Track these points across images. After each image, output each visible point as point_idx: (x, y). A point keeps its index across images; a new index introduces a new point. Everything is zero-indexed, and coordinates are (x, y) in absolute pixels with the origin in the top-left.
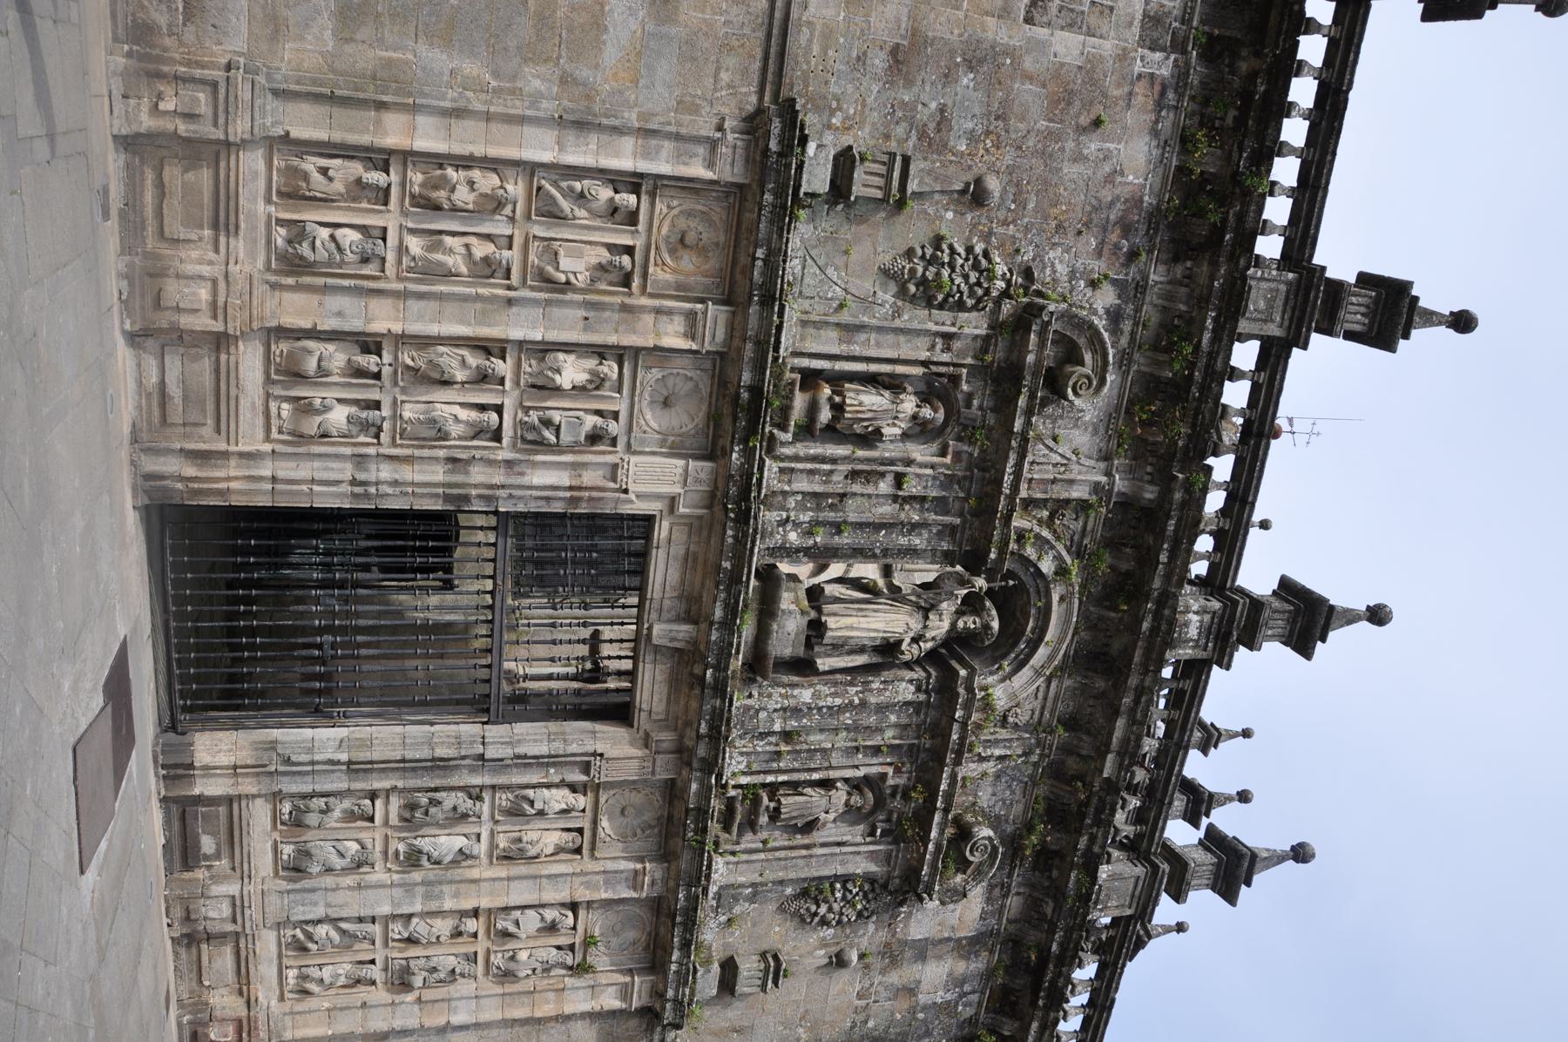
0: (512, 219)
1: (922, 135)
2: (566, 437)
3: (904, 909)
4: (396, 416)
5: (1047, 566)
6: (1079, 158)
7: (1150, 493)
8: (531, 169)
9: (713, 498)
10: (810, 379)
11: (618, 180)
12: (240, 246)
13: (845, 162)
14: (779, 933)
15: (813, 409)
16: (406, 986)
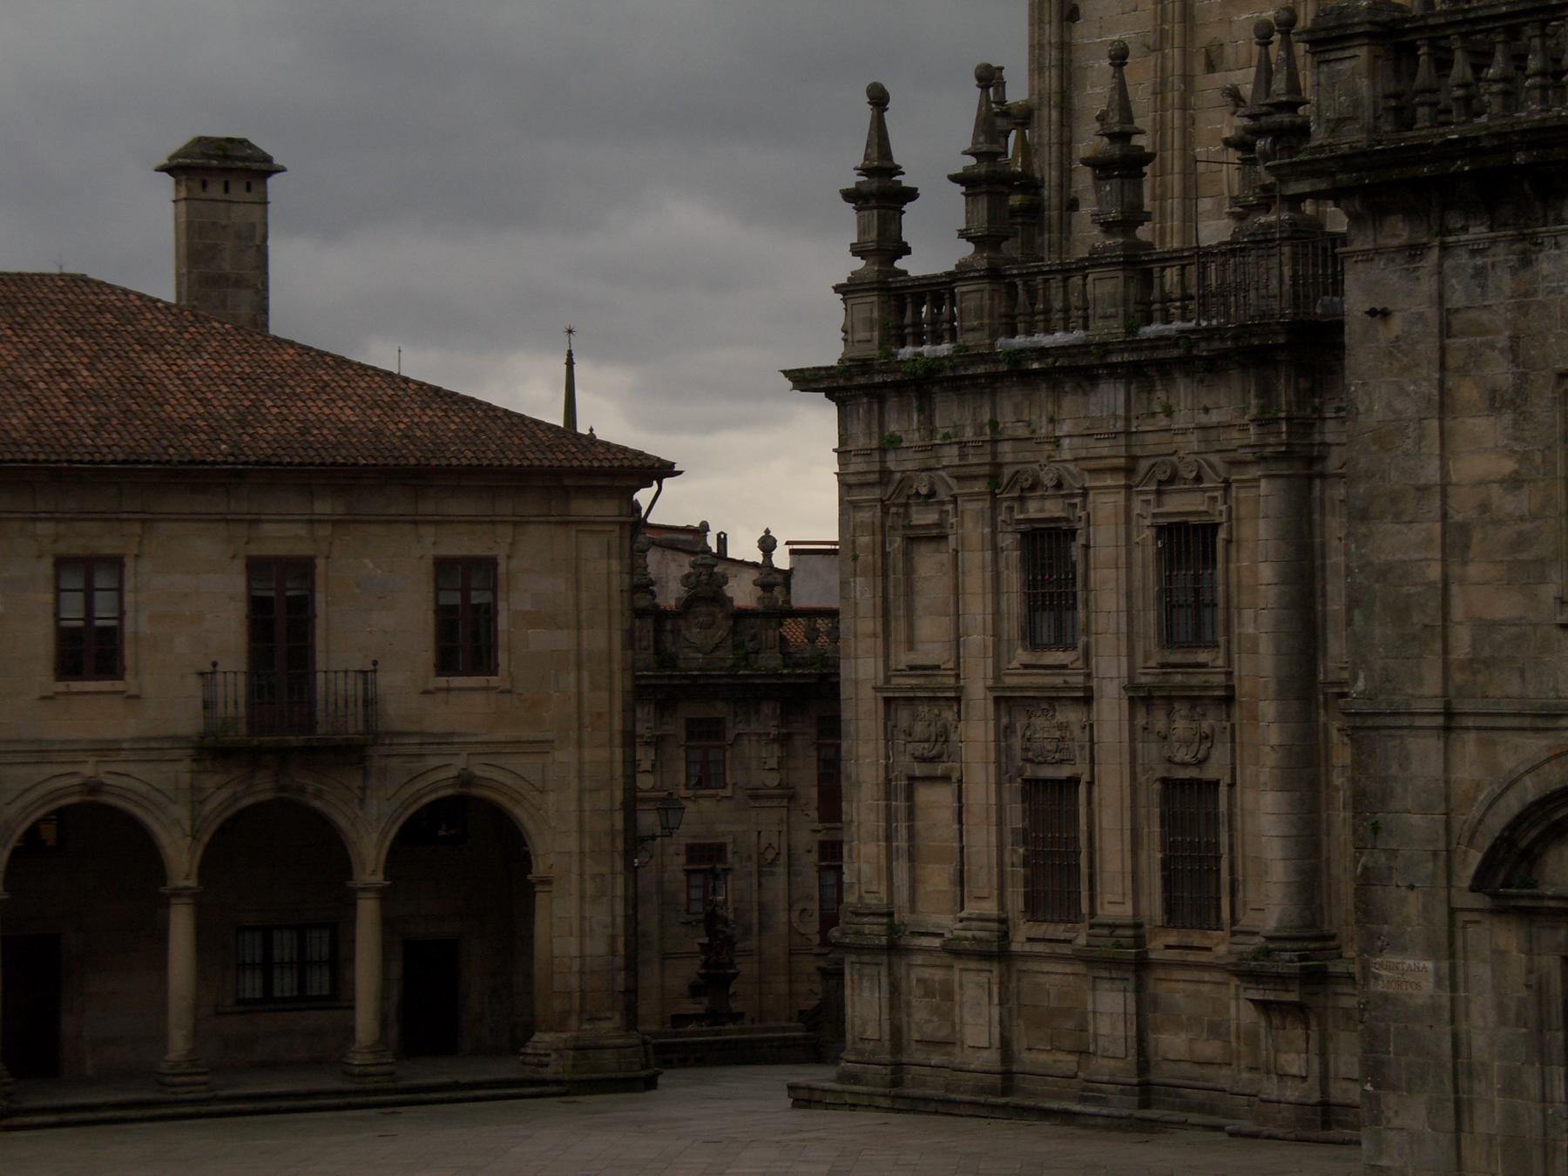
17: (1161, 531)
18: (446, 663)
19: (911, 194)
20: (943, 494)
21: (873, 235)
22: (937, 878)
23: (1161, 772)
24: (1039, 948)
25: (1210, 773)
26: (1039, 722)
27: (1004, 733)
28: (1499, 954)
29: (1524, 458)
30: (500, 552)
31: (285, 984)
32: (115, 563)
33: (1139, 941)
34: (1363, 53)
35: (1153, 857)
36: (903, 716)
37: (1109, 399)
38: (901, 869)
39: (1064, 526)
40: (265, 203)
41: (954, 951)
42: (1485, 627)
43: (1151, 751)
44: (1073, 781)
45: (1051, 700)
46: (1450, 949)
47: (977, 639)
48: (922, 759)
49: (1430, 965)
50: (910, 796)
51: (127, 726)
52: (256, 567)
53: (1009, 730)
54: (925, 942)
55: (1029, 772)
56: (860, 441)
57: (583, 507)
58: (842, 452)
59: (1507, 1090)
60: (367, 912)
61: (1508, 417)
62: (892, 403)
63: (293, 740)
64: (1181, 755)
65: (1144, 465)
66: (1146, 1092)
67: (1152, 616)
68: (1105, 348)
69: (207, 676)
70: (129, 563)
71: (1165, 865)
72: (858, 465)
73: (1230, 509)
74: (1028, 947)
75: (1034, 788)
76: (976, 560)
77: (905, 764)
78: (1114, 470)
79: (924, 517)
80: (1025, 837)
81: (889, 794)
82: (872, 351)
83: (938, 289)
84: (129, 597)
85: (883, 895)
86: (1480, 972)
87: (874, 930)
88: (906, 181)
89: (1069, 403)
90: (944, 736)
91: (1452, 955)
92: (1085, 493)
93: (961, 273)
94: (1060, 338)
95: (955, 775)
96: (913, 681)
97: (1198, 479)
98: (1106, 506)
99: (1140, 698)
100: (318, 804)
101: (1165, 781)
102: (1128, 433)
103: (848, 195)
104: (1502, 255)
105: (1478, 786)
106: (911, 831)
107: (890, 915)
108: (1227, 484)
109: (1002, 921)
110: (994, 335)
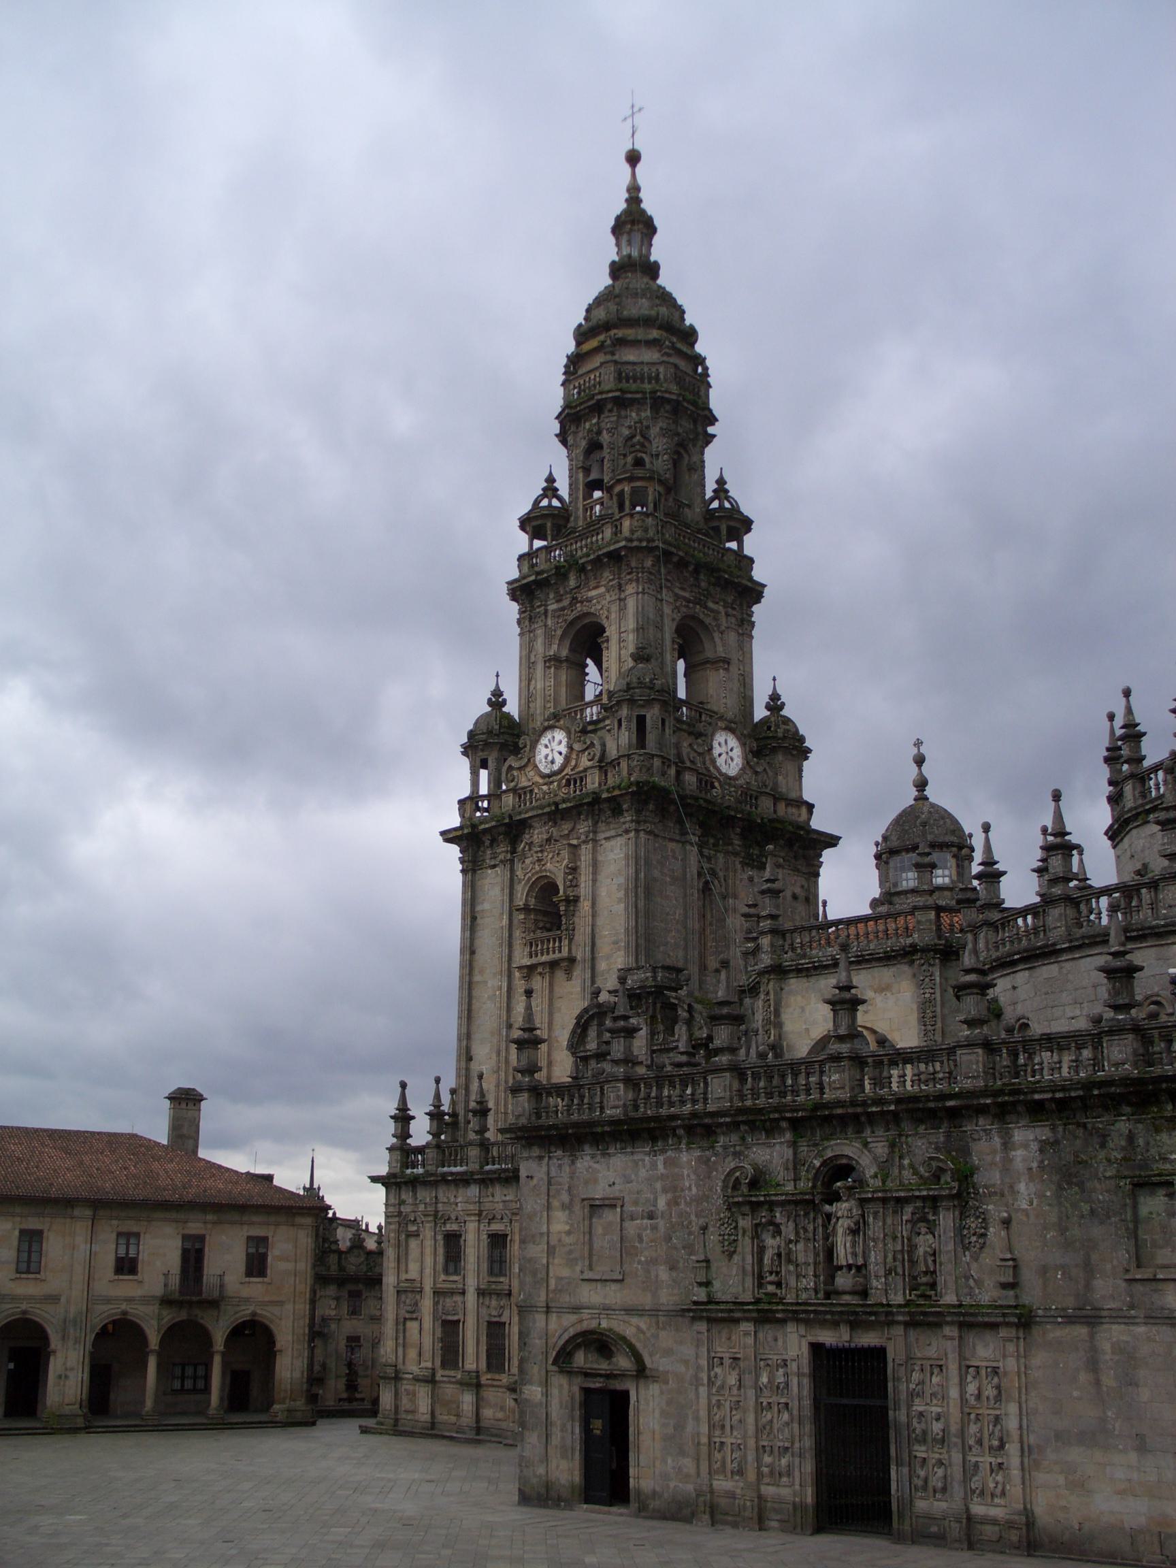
0: (726, 1400)
1: (691, 1254)
2: (781, 1380)
3: (981, 1190)
4: (782, 1440)
5: (817, 1163)
6: (690, 1189)
7: (784, 1124)
8: (710, 1395)
9: (798, 1321)
10: (760, 1286)
11: (711, 1367)
12: (738, 1491)
13: (700, 1284)
14: (988, 1259)
15: (771, 1283)
16: (1002, 1446)
17: (490, 1236)
18: (249, 1273)
19: (413, 1118)
20: (419, 1221)
21: (400, 1131)
22: (412, 1354)
23: (487, 1318)
24: (445, 1379)
25: (503, 1319)
26: (448, 1300)
27: (436, 1304)
28: (561, 1386)
29: (572, 1225)
30: (270, 1234)
31: (189, 1384)
32: (137, 1235)
33: (478, 1377)
34: (526, 1095)
35: (483, 1348)
36: (403, 1297)
37: (474, 1191)
38: (400, 1350)
40: (200, 1110)
41: (417, 1379)
42: (559, 1279)
43: (484, 1311)
44: (458, 1321)
45: (452, 1293)
46: (546, 1384)
47: (428, 1271)
48: (408, 1312)
49: (540, 1389)
50: (404, 1324)
51: (137, 1292)
52: (185, 1238)
54: (407, 1376)
56: (392, 1201)
57: (300, 1220)
58: (386, 1205)
59: (562, 1431)
60: (217, 1361)
61: (567, 1212)
62: (403, 1188)
63: (194, 1299)
64: (494, 1313)
65: (484, 1213)
66: (478, 1430)
67: (486, 1265)
68: (472, 1173)
69: (166, 1275)
70: (142, 1235)
71: (487, 1351)
72: (391, 1209)
74: (441, 1379)
75: (445, 1323)
76: (429, 1243)
77: (403, 1313)
78: (475, 1214)
79: (412, 1228)
80: (442, 1340)
81: (397, 1324)
82: (398, 1170)
83: (420, 1150)
84: (141, 1247)
86: (555, 1392)
87: (390, 1371)
88: (411, 1113)
89: (461, 1191)
90: (416, 1304)
91: (547, 1386)
92: (465, 1222)
93: (428, 1145)
94: (458, 1169)
97: (502, 1219)
98: (472, 1226)
99: (481, 1293)
100: (202, 1321)
101: (488, 1322)
102: (480, 1202)
103: (392, 1117)
104: (567, 1161)
105: (556, 1331)
106: (404, 1337)
107: (396, 1366)
108: (511, 1220)
109: (433, 1369)
110: (437, 1167)
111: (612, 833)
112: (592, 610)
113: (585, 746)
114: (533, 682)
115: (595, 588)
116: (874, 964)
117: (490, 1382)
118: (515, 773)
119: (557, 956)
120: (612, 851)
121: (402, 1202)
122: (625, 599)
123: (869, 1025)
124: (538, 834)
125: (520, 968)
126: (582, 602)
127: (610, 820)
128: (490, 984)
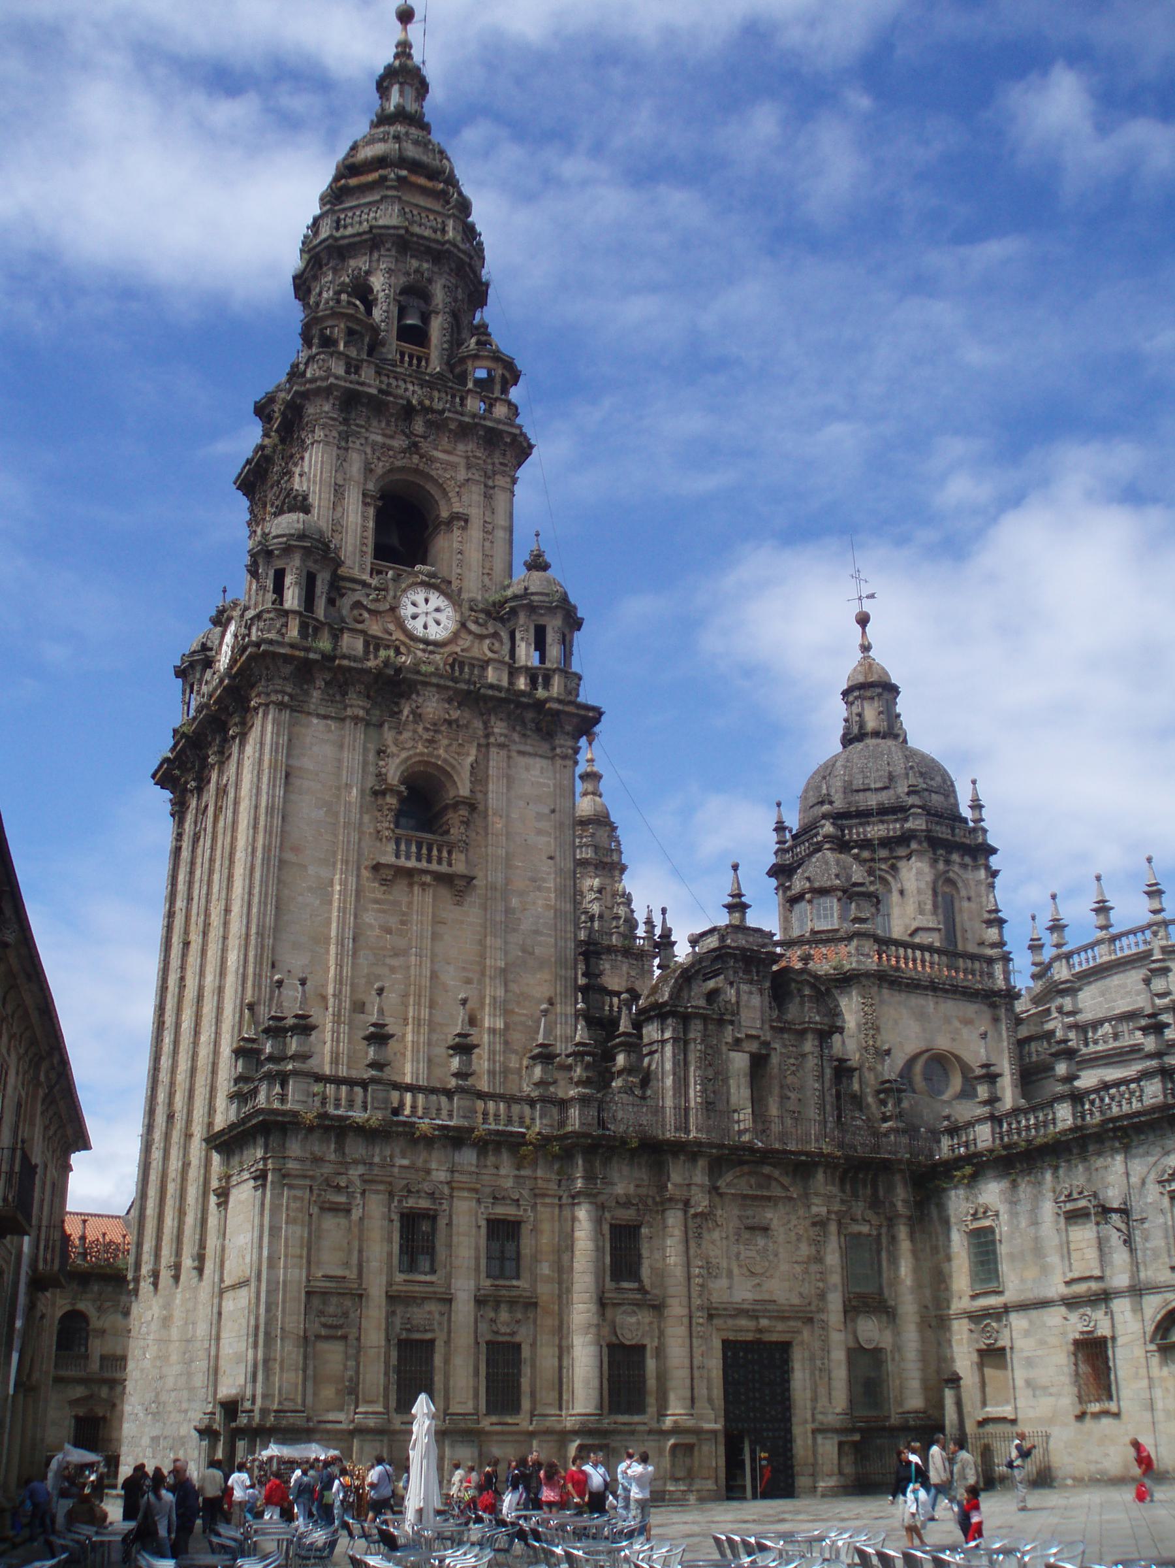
23: (489, 1337)
25: (517, 1339)
27: (391, 1314)
36: (316, 1302)
37: (467, 1157)
38: (310, 1384)
39: (432, 1213)
48: (325, 1326)
53: (393, 1313)
55: (404, 1335)
73: (535, 1217)
85: (299, 1401)
90: (346, 1315)
95: (351, 1337)
96: (328, 1284)
99: (480, 1302)
101: (488, 1343)
111: (528, 749)
112: (433, 473)
113: (485, 632)
114: (340, 509)
115: (444, 451)
116: (957, 997)
117: (498, 1428)
118: (366, 615)
119: (444, 868)
120: (527, 769)
121: (318, 1160)
122: (494, 487)
123: (957, 1052)
124: (432, 706)
125: (376, 868)
126: (421, 457)
127: (529, 733)
128: (311, 870)
